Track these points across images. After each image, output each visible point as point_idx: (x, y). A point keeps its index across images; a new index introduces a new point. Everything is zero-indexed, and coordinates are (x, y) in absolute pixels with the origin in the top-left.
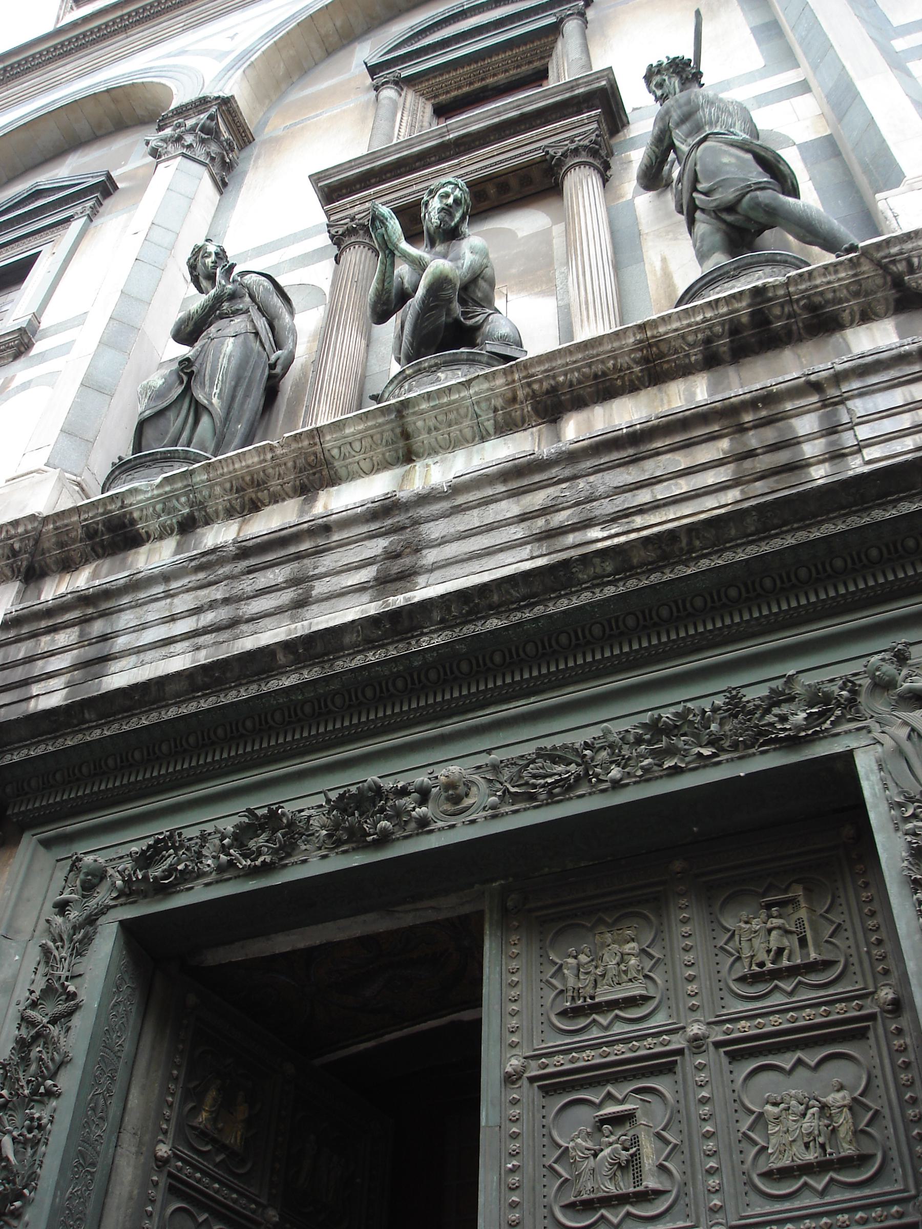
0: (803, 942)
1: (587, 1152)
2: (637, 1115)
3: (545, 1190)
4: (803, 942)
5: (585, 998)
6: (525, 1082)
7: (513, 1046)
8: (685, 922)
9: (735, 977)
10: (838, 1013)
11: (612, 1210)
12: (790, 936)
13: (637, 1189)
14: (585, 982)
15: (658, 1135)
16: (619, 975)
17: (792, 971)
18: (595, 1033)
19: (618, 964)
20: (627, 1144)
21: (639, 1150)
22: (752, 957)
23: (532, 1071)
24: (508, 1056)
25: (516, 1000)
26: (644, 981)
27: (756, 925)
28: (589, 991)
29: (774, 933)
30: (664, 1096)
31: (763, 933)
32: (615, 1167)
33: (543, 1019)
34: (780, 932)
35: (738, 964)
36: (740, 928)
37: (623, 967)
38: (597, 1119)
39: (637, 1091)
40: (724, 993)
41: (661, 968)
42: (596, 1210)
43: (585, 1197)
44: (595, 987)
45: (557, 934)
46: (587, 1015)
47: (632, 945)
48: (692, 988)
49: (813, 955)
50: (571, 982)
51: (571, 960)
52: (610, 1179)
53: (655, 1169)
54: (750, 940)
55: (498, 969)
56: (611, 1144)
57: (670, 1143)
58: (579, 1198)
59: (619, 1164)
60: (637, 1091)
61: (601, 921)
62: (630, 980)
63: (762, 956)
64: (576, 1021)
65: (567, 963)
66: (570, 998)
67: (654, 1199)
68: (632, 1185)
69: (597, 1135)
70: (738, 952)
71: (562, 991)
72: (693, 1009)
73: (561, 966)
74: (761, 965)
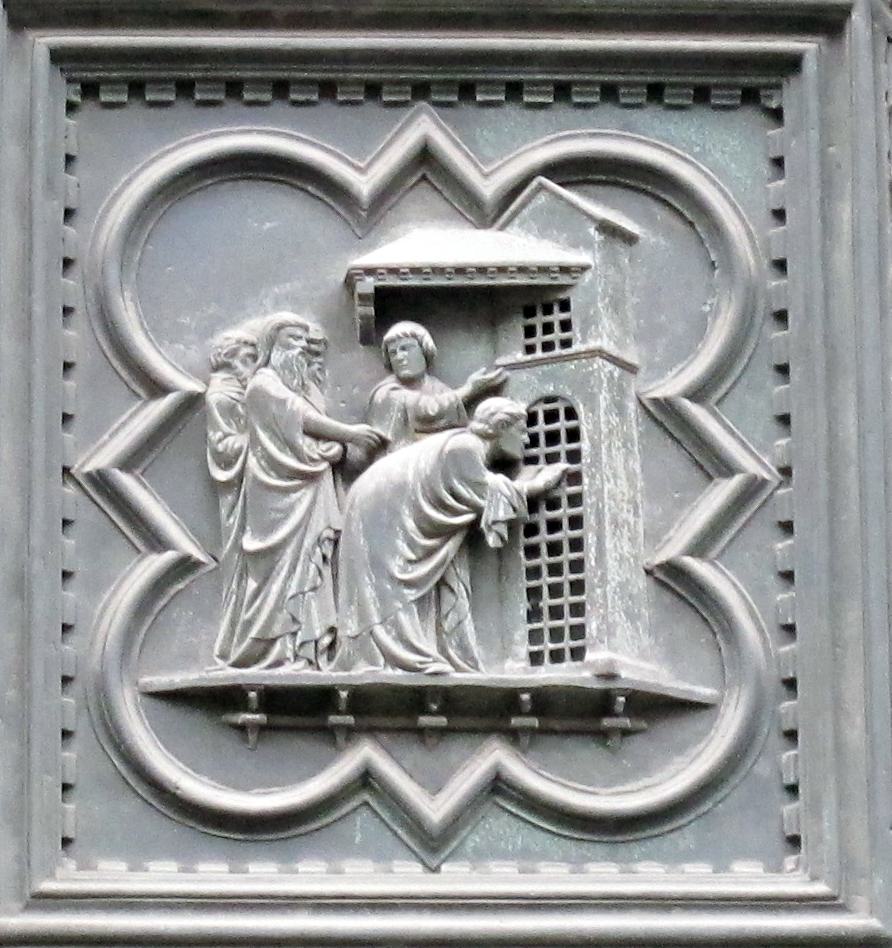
1: (307, 444)
2: (576, 299)
3: (71, 594)
11: (415, 753)
13: (551, 674)
15: (665, 417)
20: (515, 444)
21: (574, 478)
30: (716, 228)
32: (450, 547)
38: (368, 285)
39: (574, 171)
42: (335, 739)
43: (294, 672)
52: (420, 601)
53: (642, 583)
56: (428, 424)
57: (727, 468)
58: (257, 673)
59: (473, 536)
60: (574, 171)
67: (626, 733)
68: (524, 649)
69: (360, 357)
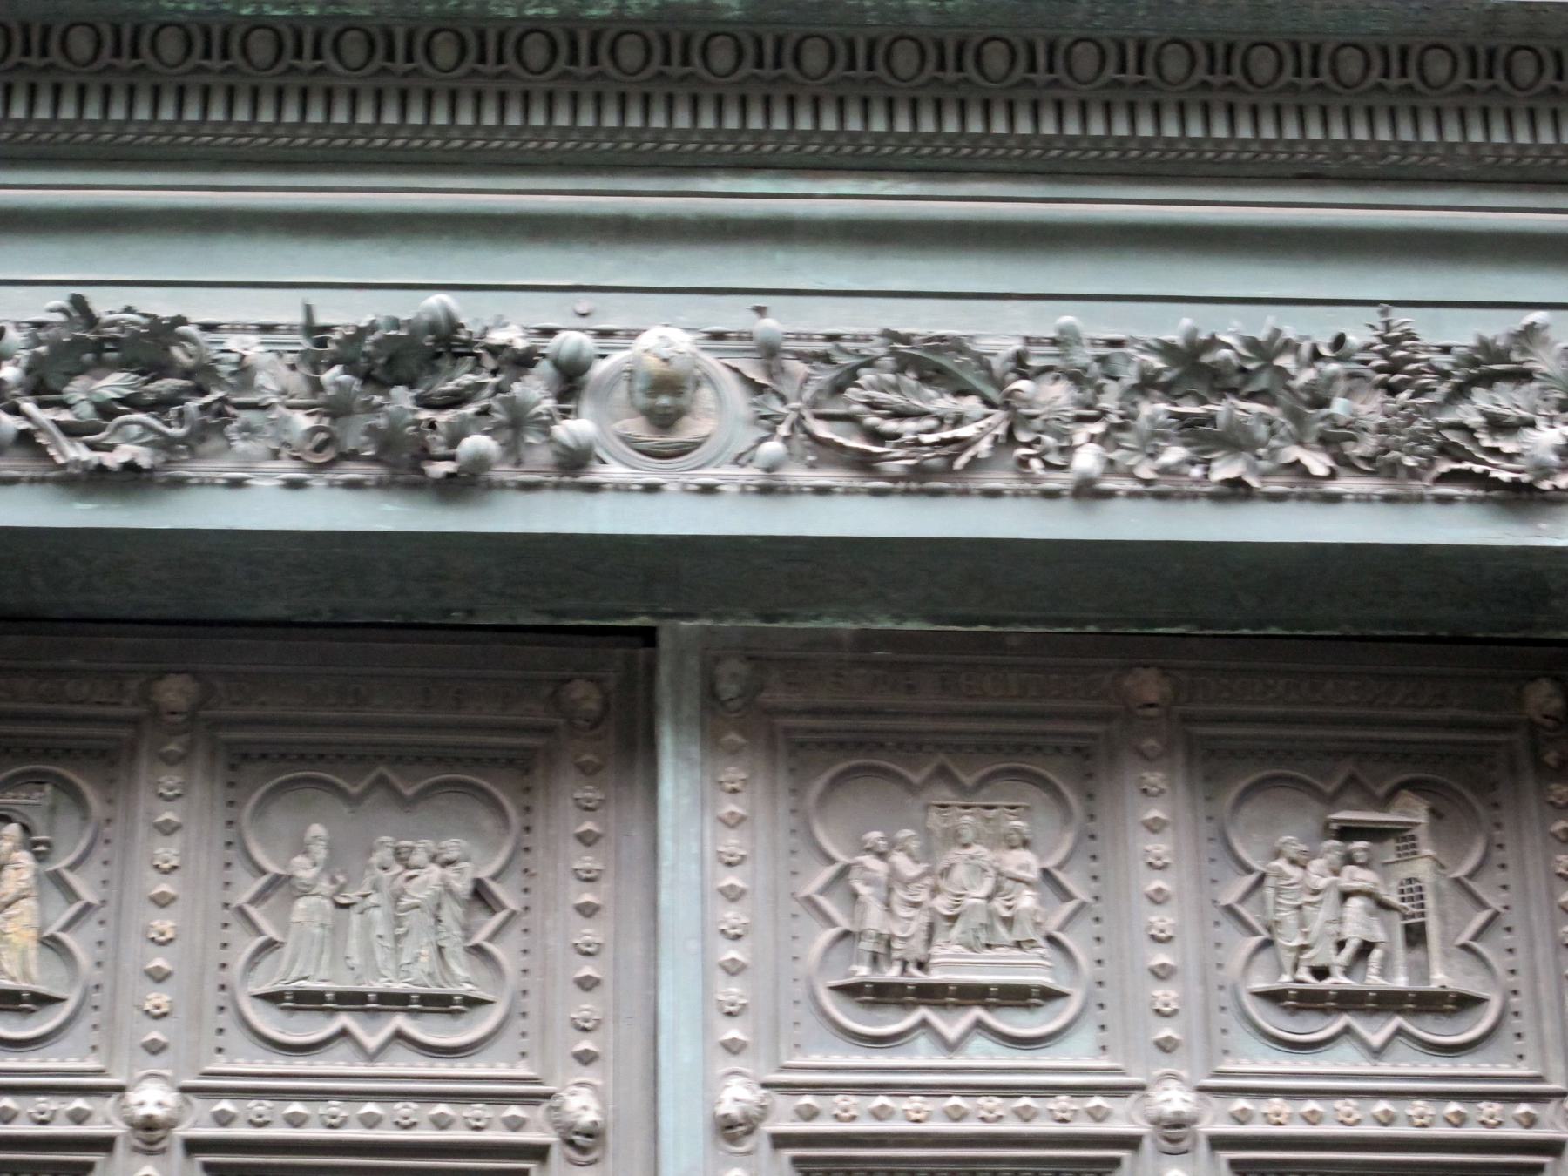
0: (1415, 936)
4: (1415, 936)
5: (905, 963)
6: (759, 1141)
7: (733, 1048)
8: (1154, 827)
9: (1261, 984)
10: (1483, 1123)
12: (1383, 913)
14: (908, 926)
16: (988, 927)
17: (1388, 1003)
18: (921, 1054)
19: (989, 898)
22: (1303, 948)
23: (778, 1120)
24: (722, 1070)
25: (738, 937)
26: (1045, 949)
27: (1318, 874)
28: (917, 950)
29: (1355, 903)
31: (1333, 897)
33: (800, 991)
34: (1369, 903)
35: (1265, 957)
36: (1281, 875)
37: (999, 904)
40: (1230, 1019)
41: (1086, 927)
44: (929, 941)
45: (835, 782)
46: (908, 1007)
47: (1024, 856)
48: (1165, 994)
49: (1440, 978)
50: (874, 919)
51: (870, 861)
54: (1299, 907)
55: (695, 849)
61: (943, 774)
62: (1018, 945)
63: (1321, 953)
64: (879, 1014)
65: (865, 869)
66: (867, 957)
70: (1269, 930)
71: (846, 934)
72: (1165, 1046)
73: (845, 871)
74: (1321, 973)
